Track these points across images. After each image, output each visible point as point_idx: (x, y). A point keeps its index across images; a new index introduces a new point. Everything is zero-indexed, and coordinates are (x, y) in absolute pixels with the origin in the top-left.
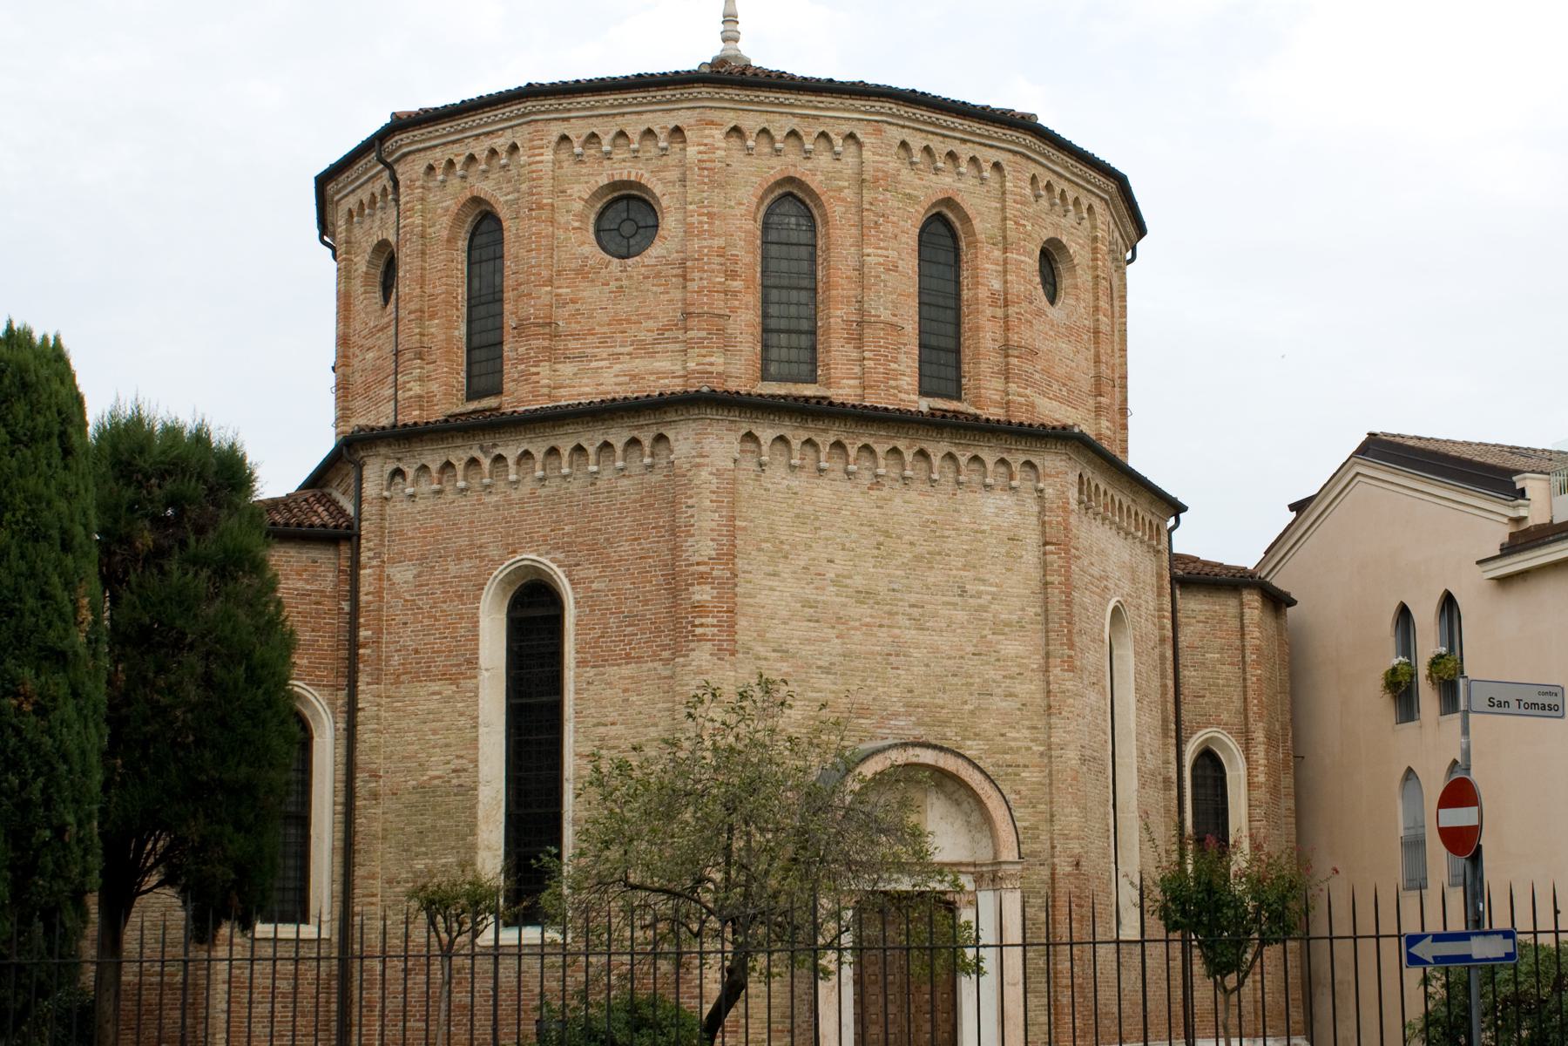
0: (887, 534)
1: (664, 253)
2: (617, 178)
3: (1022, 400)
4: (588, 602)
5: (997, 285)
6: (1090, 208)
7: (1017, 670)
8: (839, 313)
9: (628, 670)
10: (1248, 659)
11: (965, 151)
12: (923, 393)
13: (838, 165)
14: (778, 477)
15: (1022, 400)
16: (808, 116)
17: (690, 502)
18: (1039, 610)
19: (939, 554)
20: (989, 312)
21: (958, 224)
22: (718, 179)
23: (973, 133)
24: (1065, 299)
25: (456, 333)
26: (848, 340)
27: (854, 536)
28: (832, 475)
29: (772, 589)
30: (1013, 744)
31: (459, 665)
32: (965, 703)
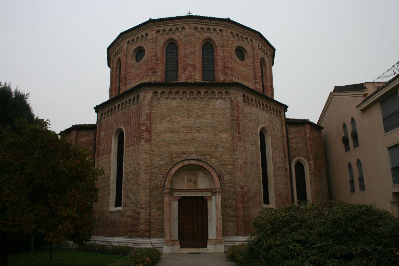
0: (190, 111)
1: (145, 59)
2: (138, 46)
3: (229, 79)
4: (127, 134)
5: (222, 55)
6: (251, 40)
7: (225, 141)
8: (181, 64)
9: (132, 148)
10: (307, 140)
11: (212, 28)
12: (203, 80)
13: (181, 34)
14: (163, 101)
15: (229, 79)
16: (174, 25)
17: (142, 108)
18: (231, 126)
19: (204, 115)
20: (220, 61)
21: (213, 44)
22: (156, 41)
23: (213, 23)
24: (246, 60)
25: (117, 85)
26: (183, 70)
27: (182, 112)
28: (176, 99)
29: (161, 126)
30: (224, 159)
31: (109, 151)
32: (211, 150)
